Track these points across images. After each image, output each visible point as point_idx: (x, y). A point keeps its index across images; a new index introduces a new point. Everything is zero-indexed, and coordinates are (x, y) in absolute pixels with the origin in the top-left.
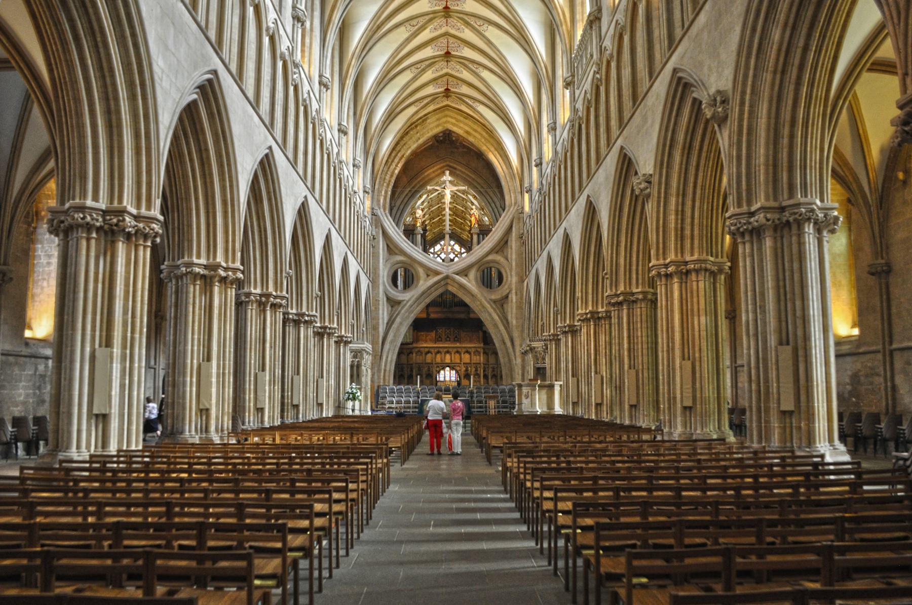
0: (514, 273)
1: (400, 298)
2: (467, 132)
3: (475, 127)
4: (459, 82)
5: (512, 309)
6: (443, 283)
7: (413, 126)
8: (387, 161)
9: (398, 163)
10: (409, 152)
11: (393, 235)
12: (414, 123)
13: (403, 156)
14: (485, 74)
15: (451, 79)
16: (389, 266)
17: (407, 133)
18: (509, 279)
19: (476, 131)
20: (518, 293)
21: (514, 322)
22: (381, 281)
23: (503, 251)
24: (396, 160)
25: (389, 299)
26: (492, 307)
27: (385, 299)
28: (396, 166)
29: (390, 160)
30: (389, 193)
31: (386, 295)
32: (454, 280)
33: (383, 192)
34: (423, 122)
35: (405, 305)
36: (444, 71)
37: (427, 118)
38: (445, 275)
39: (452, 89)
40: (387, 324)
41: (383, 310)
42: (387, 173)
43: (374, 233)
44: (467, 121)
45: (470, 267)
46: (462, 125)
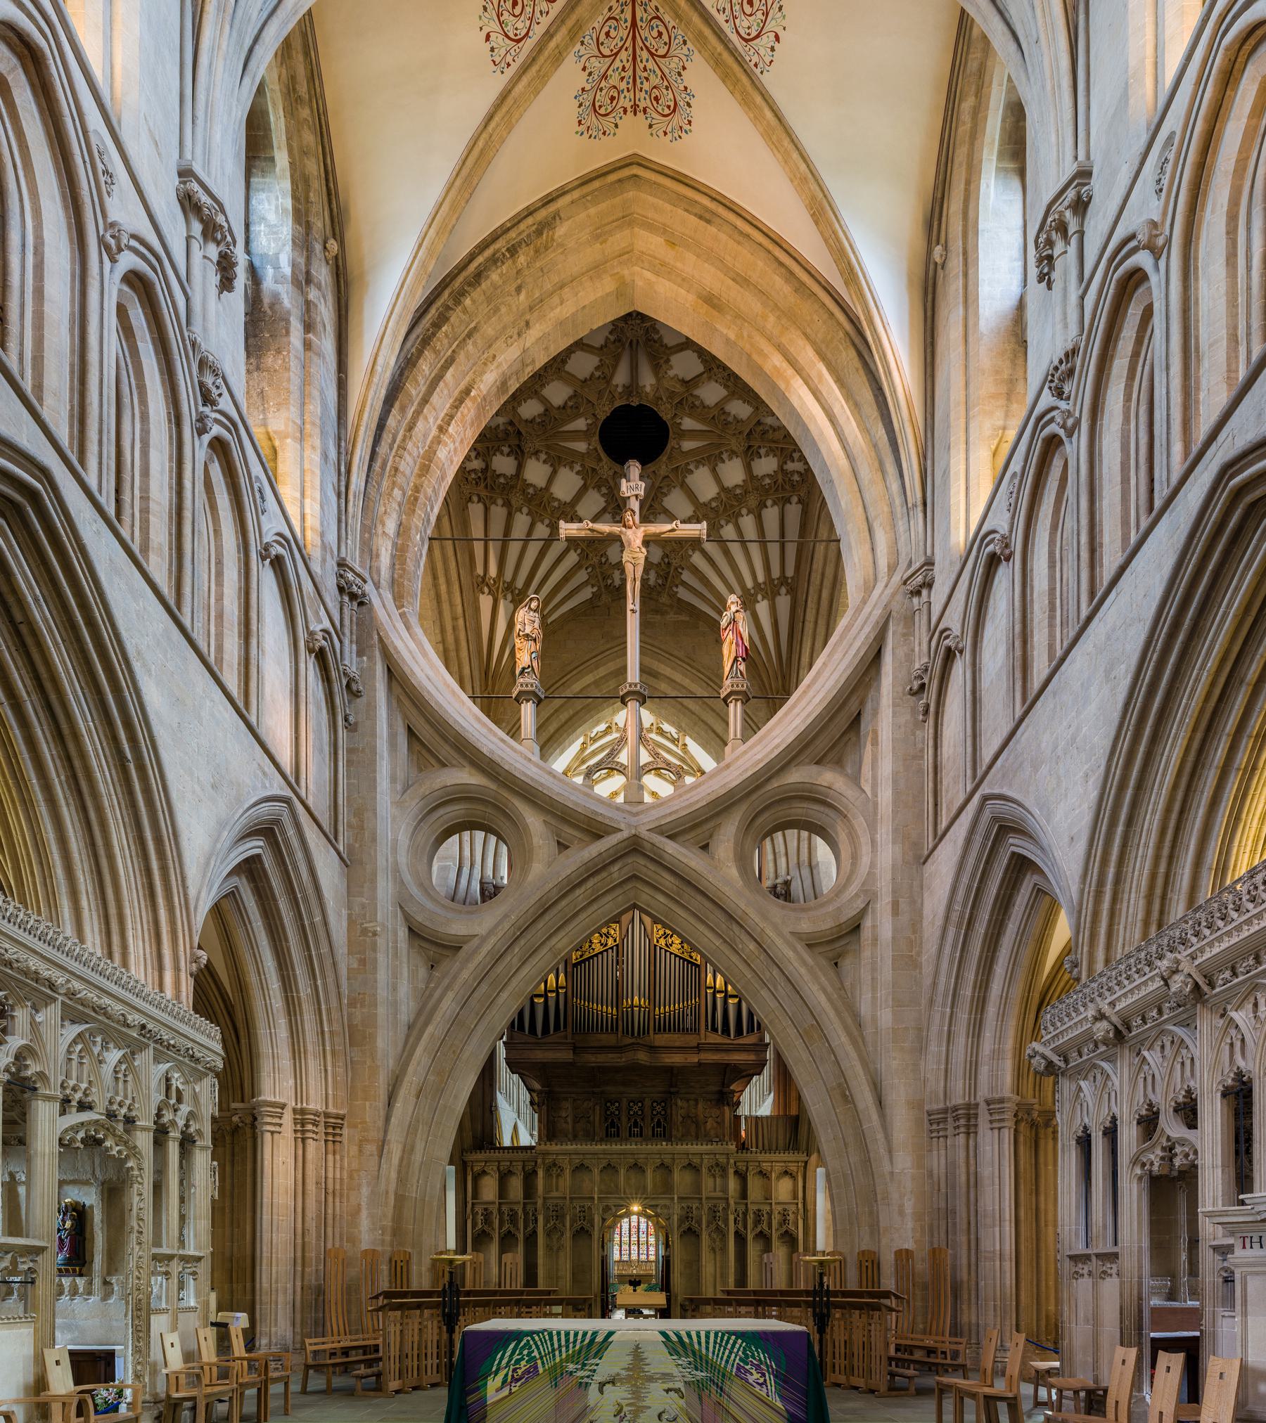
0: (885, 833)
5: (874, 970)
6: (617, 872)
7: (501, 244)
17: (478, 276)
20: (903, 906)
21: (886, 1017)
25: (414, 933)
26: (804, 963)
29: (414, 390)
32: (657, 860)
34: (539, 233)
35: (476, 951)
37: (556, 216)
38: (625, 834)
41: (395, 975)
45: (721, 807)
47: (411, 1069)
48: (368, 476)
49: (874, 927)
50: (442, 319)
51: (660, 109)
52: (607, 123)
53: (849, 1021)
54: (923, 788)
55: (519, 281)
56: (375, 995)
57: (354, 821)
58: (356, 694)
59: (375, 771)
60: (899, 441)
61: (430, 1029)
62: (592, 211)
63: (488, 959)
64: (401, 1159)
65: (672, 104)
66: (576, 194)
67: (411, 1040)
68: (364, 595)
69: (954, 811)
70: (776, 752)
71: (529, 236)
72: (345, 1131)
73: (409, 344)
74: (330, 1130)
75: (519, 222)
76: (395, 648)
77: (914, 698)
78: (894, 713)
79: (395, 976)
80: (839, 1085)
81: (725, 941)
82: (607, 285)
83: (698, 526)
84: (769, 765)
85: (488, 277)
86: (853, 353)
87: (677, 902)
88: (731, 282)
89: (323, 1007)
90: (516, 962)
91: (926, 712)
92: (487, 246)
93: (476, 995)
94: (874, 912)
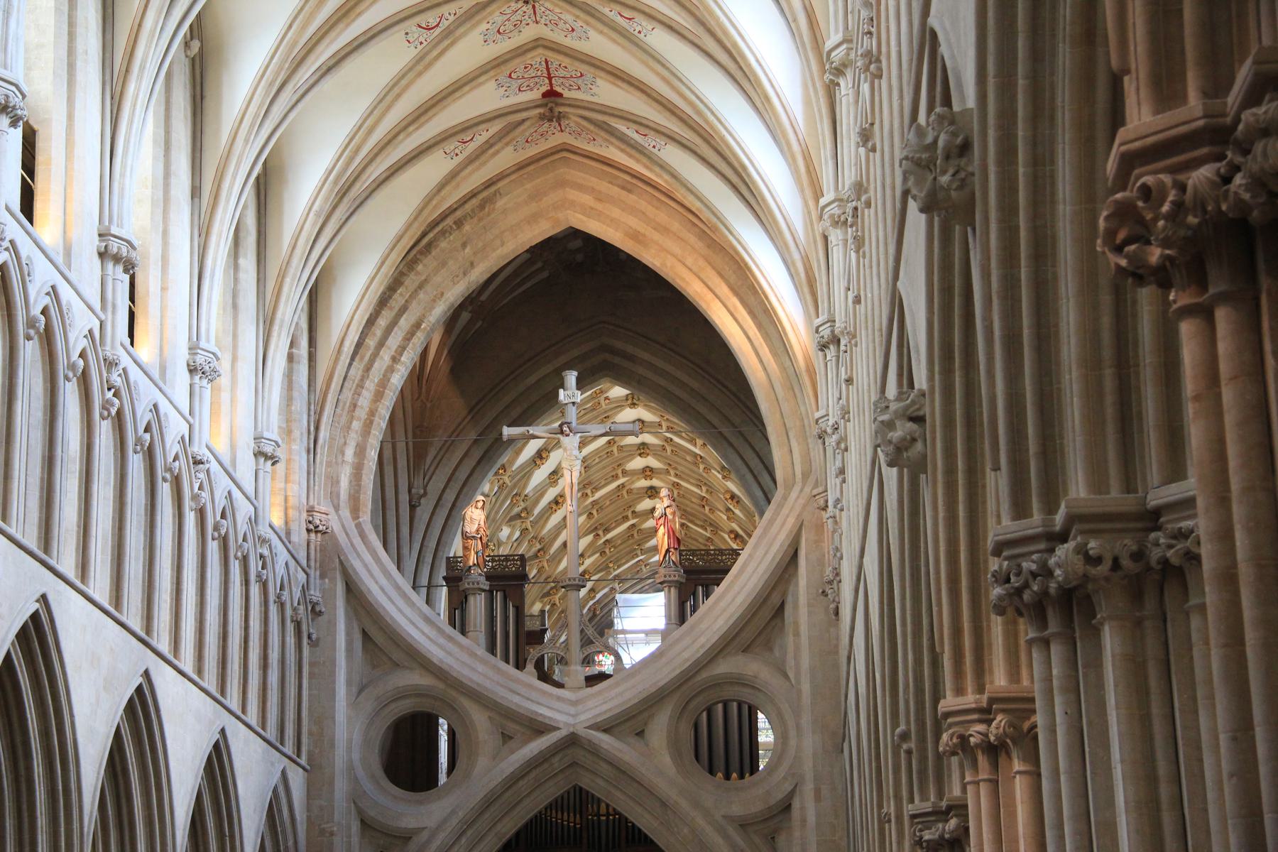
0: (806, 719)
1: (408, 822)
2: (636, 236)
3: (662, 217)
4: (584, 68)
7: (449, 221)
8: (359, 345)
9: (402, 349)
12: (452, 210)
13: (417, 326)
14: (659, 40)
15: (555, 59)
17: (429, 246)
18: (793, 742)
19: (665, 230)
23: (768, 646)
24: (394, 341)
27: (355, 827)
28: (395, 359)
29: (371, 342)
30: (373, 455)
31: (360, 812)
32: (594, 751)
34: (482, 207)
36: (529, 33)
37: (497, 192)
39: (566, 94)
42: (361, 386)
43: (315, 594)
44: (631, 199)
46: (616, 212)
55: (465, 239)
58: (320, 613)
59: (334, 682)
62: (528, 186)
66: (513, 177)
70: (702, 651)
71: (473, 210)
75: (465, 202)
76: (354, 570)
78: (810, 614)
84: (697, 662)
85: (438, 245)
92: (437, 224)
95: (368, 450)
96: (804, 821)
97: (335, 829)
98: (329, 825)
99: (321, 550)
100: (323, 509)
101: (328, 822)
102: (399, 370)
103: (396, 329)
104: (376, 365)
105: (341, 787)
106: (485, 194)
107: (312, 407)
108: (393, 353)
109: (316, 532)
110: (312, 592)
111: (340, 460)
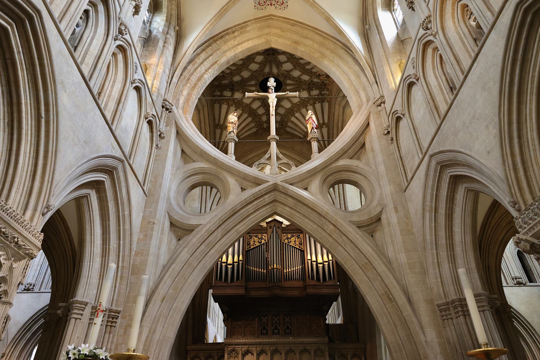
0: (384, 181)
1: (194, 221)
2: (296, 43)
3: (306, 32)
6: (267, 198)
10: (224, 60)
11: (191, 134)
12: (231, 28)
13: (216, 62)
16: (180, 176)
17: (222, 37)
18: (378, 193)
19: (307, 38)
20: (399, 208)
21: (403, 258)
22: (162, 195)
24: (207, 64)
29: (198, 61)
31: (170, 217)
33: (185, 93)
34: (242, 28)
38: (271, 183)
40: (164, 267)
42: (192, 74)
47: (160, 286)
48: (179, 79)
49: (387, 218)
50: (210, 45)
51: (278, 4)
52: (263, 7)
53: (385, 260)
54: (397, 165)
56: (148, 251)
57: (153, 179)
60: (364, 68)
61: (174, 266)
62: (258, 25)
63: (206, 234)
64: (147, 337)
65: (282, 3)
66: (253, 21)
67: (163, 272)
68: (171, 109)
69: (413, 172)
72: (119, 321)
73: (198, 50)
74: (111, 319)
76: (181, 124)
77: (386, 136)
79: (161, 242)
80: (386, 292)
81: (318, 226)
82: (262, 40)
83: (295, 93)
86: (344, 51)
87: (295, 210)
88: (302, 38)
89: (121, 254)
90: (219, 236)
91: (392, 139)
92: (226, 31)
93: (198, 250)
94: (386, 212)
95: (193, 95)
96: (389, 224)
97: (156, 221)
98: (153, 220)
99: (167, 118)
100: (170, 101)
101: (153, 218)
102: (207, 74)
103: (208, 60)
104: (199, 69)
105: (162, 207)
106: (243, 25)
107: (171, 71)
108: (206, 69)
109: (167, 109)
110: (161, 127)
111: (181, 93)
